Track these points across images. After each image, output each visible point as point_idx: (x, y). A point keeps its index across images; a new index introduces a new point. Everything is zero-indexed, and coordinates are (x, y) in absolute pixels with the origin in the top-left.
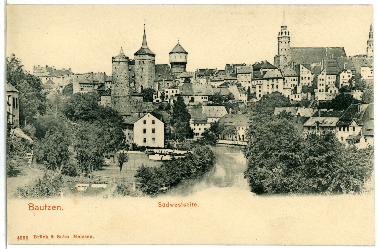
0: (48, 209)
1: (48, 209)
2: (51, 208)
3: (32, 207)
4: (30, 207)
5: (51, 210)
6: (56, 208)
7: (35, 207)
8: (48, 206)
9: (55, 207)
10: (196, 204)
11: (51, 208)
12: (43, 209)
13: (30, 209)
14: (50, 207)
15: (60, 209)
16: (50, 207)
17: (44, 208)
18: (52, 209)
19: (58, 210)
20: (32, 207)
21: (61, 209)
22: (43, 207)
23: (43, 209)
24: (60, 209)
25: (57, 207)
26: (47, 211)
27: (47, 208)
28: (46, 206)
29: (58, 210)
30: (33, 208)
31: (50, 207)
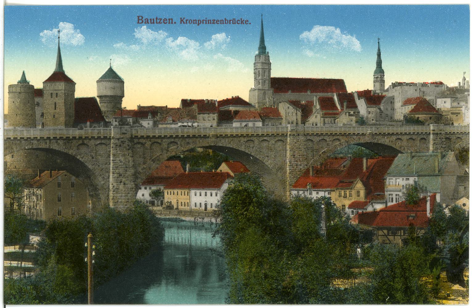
0: (159, 22)
1: (159, 22)
2: (162, 21)
3: (142, 20)
4: (139, 20)
5: (161, 23)
9: (167, 20)
11: (162, 21)
14: (161, 19)
15: (172, 23)
16: (161, 19)
18: (163, 23)
23: (154, 23)
27: (158, 21)
28: (157, 19)
31: (161, 20)
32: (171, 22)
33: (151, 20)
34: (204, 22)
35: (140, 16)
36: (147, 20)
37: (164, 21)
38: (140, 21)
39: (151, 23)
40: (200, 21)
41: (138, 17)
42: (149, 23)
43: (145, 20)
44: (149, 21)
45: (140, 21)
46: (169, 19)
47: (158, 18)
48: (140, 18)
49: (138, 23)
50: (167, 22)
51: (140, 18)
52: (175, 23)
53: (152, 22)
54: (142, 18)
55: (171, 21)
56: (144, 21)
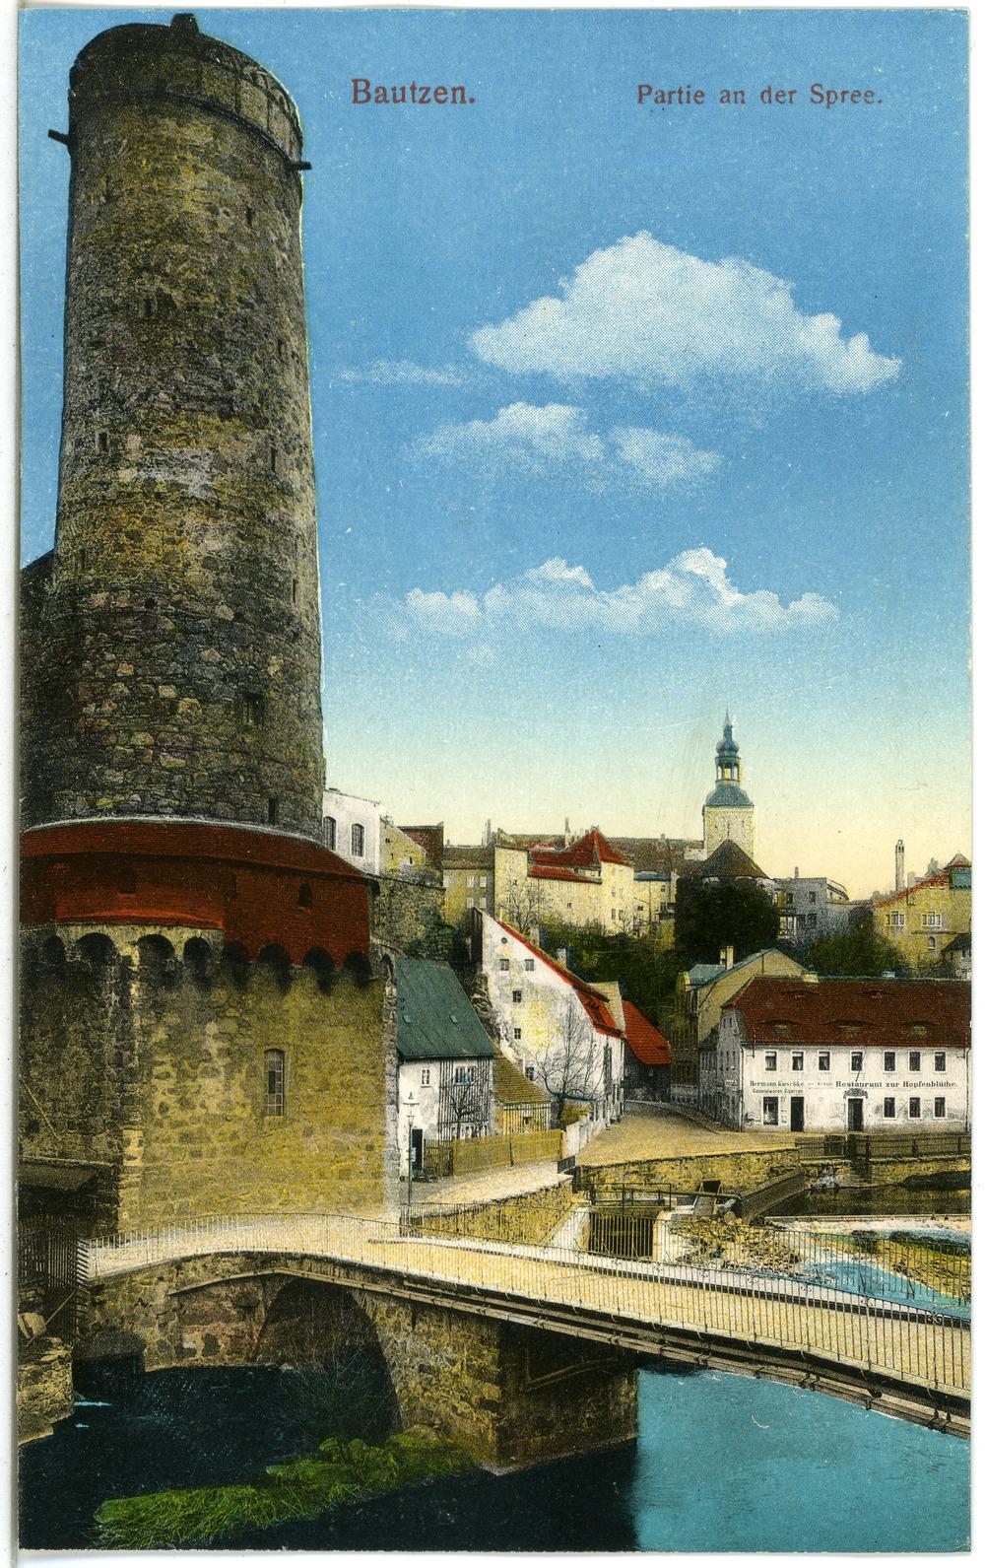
0: (421, 101)
1: (421, 101)
2: (431, 95)
3: (365, 91)
4: (356, 91)
6: (450, 95)
7: (372, 90)
8: (421, 89)
9: (445, 93)
10: (873, 94)
12: (403, 100)
13: (359, 99)
14: (428, 89)
15: (463, 101)
16: (428, 89)
17: (408, 92)
18: (433, 98)
19: (454, 101)
20: (365, 91)
21: (467, 99)
22: (403, 89)
23: (403, 100)
24: (463, 101)
25: (450, 92)
26: (417, 105)
27: (419, 95)
28: (413, 88)
29: (454, 101)
30: (369, 96)
31: (426, 93)
32: (458, 99)
33: (394, 89)
34: (675, 96)
35: (360, 80)
36: (381, 91)
37: (436, 93)
38: (362, 96)
39: (395, 101)
40: (832, 95)
41: (356, 81)
42: (387, 102)
43: (377, 91)
44: (390, 97)
45: (362, 96)
46: (454, 90)
47: (418, 86)
48: (362, 86)
49: (355, 101)
50: (447, 99)
51: (362, 86)
52: (472, 101)
53: (399, 97)
54: (368, 84)
55: (459, 93)
56: (374, 95)
